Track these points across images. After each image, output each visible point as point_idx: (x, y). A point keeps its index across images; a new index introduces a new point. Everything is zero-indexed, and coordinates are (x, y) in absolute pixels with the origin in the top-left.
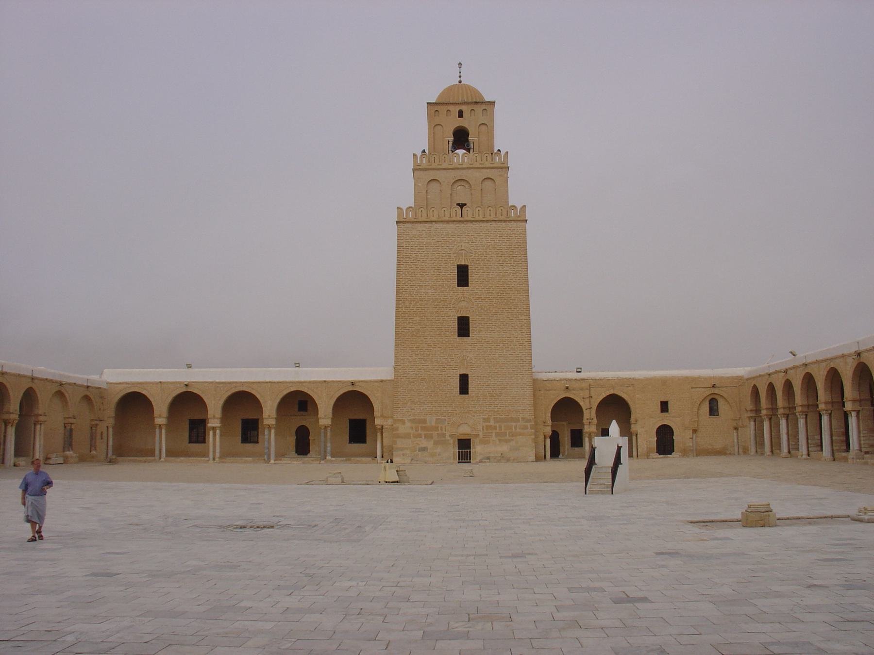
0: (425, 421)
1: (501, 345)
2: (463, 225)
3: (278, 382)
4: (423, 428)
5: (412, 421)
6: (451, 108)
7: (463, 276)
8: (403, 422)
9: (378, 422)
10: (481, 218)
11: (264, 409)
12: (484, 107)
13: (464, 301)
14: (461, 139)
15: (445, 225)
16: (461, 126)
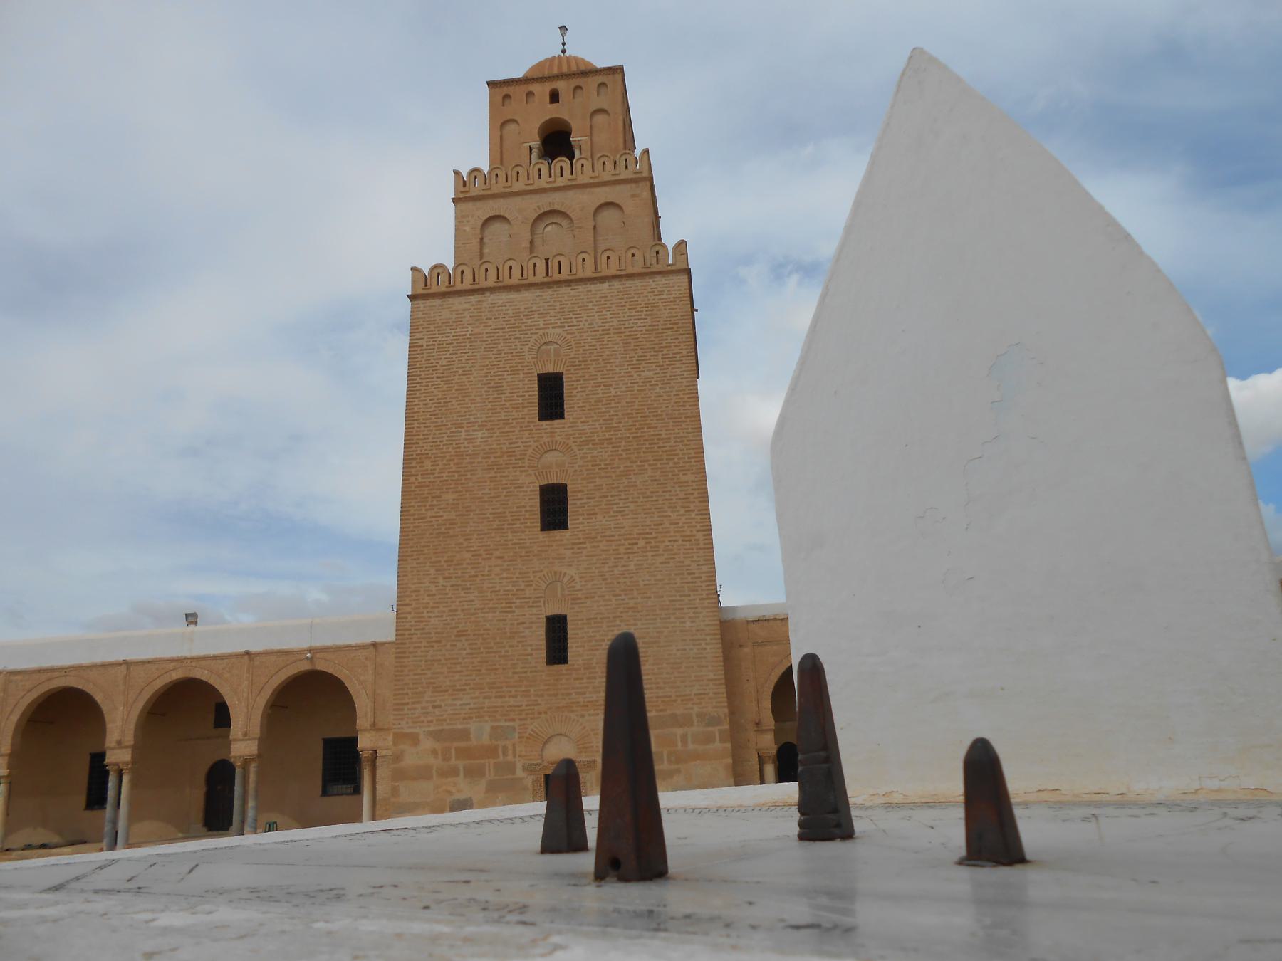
0: (465, 735)
1: (642, 543)
2: (550, 292)
3: (144, 663)
4: (462, 753)
5: (436, 735)
6: (535, 88)
7: (551, 396)
8: (414, 739)
9: (365, 742)
10: (589, 273)
11: (109, 726)
12: (600, 79)
13: (559, 452)
14: (556, 142)
15: (514, 296)
16: (560, 125)
